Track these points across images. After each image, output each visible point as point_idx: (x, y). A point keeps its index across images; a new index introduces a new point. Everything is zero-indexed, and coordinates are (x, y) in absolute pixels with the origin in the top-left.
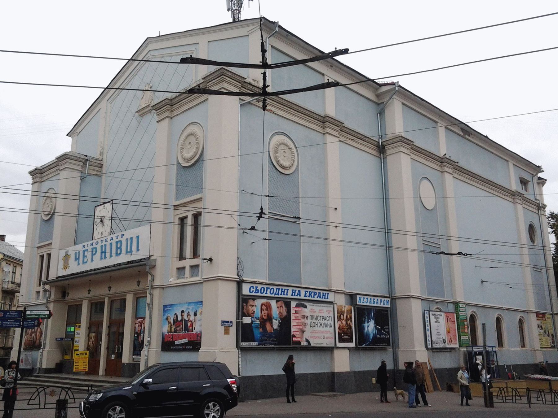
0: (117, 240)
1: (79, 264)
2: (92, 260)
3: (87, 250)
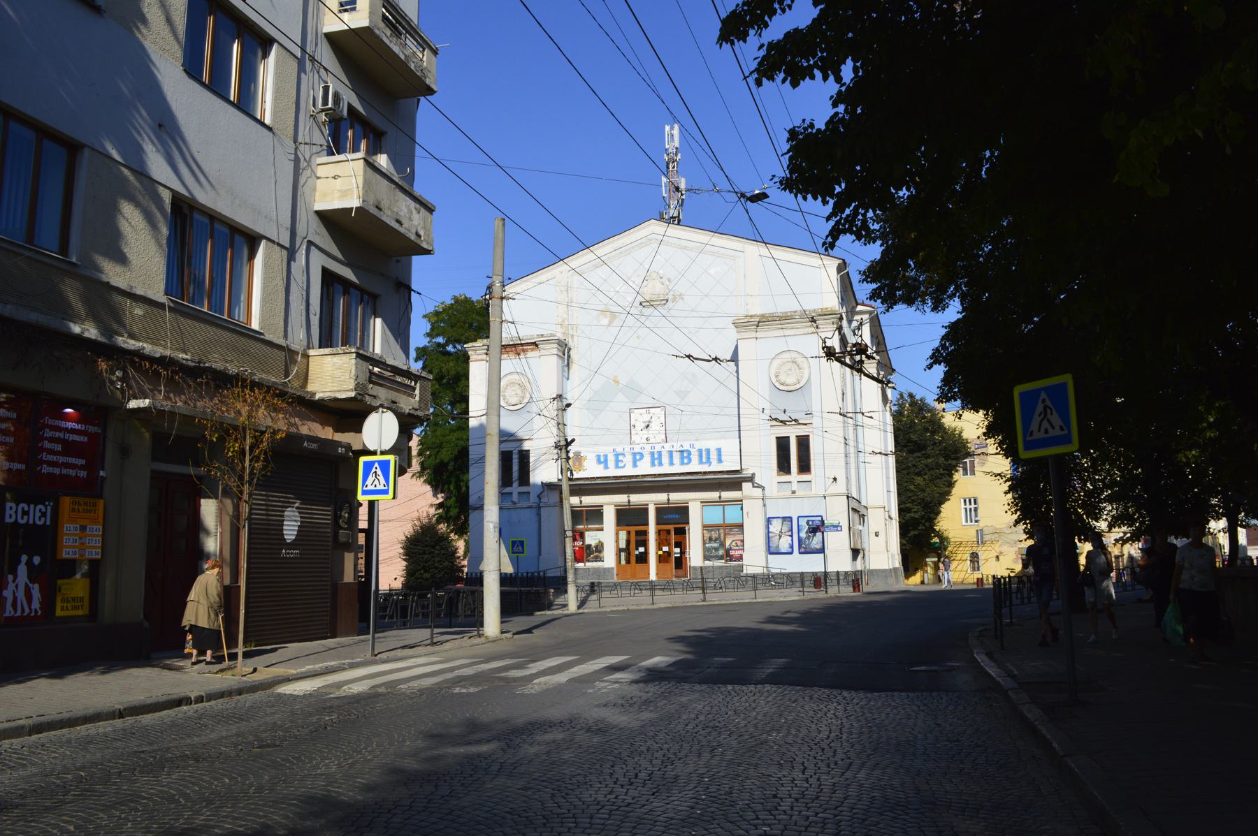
1: (606, 467)
2: (635, 465)
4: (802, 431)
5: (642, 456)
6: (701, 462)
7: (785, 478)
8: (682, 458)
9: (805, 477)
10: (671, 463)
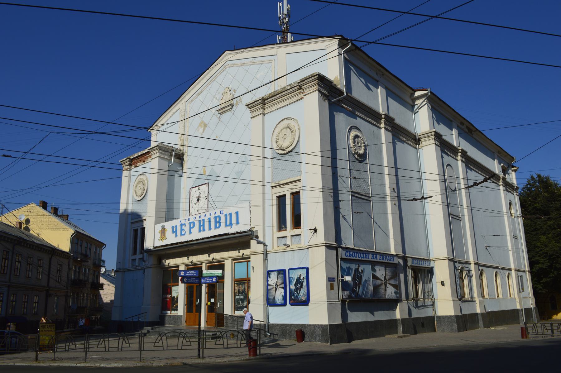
0: (216, 215)
1: (176, 236)
2: (190, 233)
3: (185, 224)
4: (294, 188)
7: (282, 234)
8: (216, 222)
9: (297, 231)
10: (210, 229)
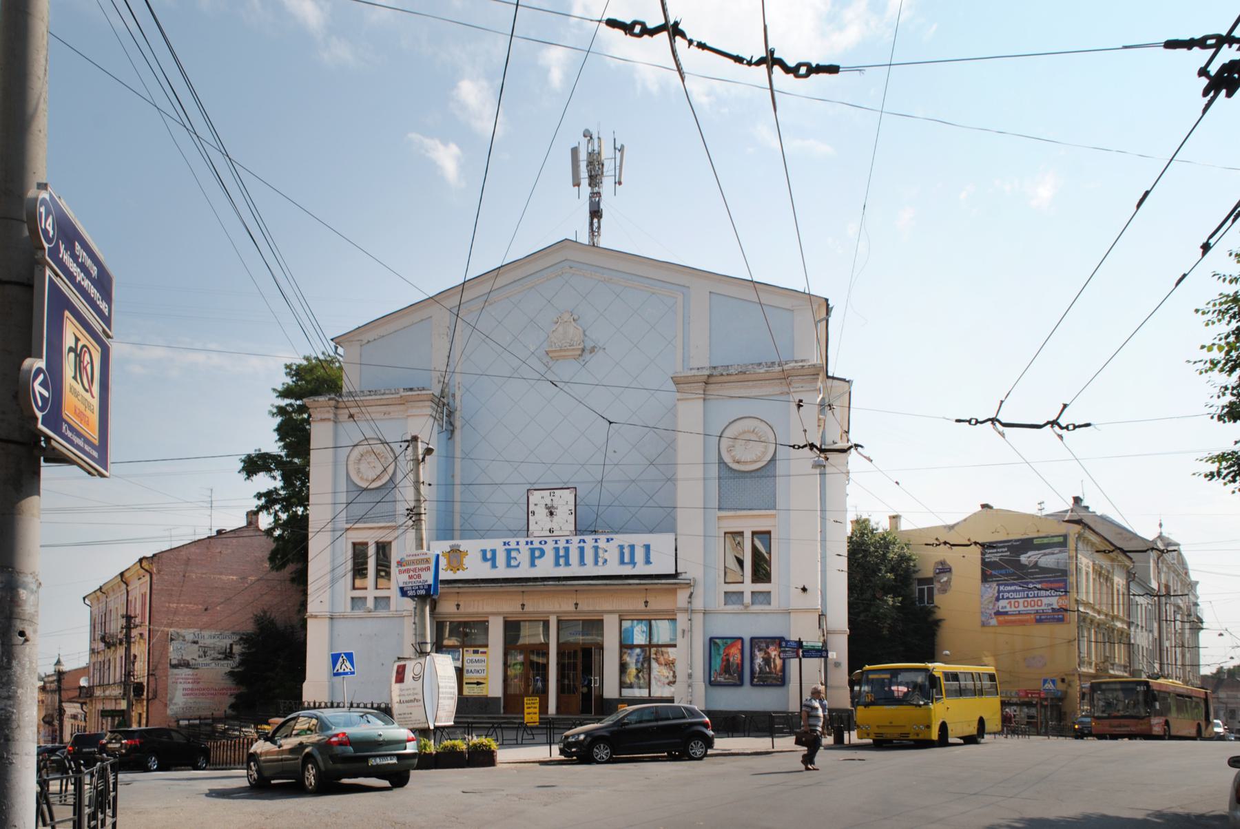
1: (494, 566)
2: (533, 564)
5: (543, 553)
6: (622, 562)
10: (582, 562)
